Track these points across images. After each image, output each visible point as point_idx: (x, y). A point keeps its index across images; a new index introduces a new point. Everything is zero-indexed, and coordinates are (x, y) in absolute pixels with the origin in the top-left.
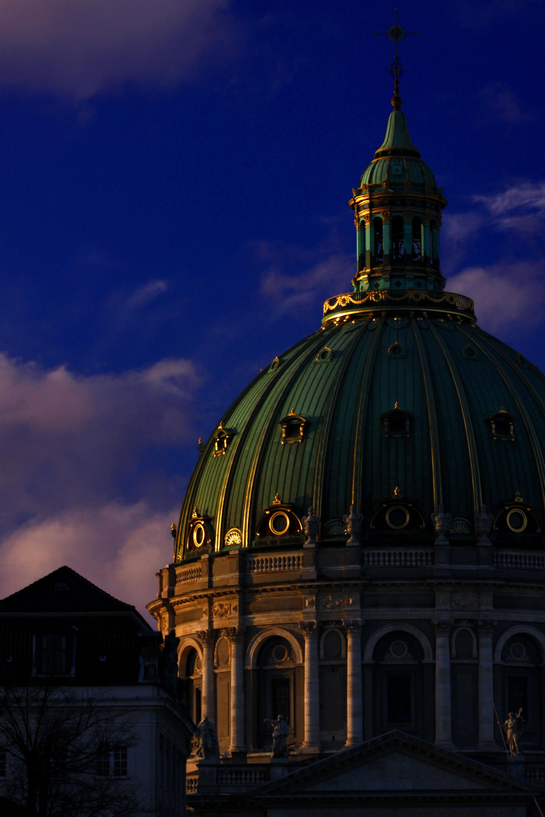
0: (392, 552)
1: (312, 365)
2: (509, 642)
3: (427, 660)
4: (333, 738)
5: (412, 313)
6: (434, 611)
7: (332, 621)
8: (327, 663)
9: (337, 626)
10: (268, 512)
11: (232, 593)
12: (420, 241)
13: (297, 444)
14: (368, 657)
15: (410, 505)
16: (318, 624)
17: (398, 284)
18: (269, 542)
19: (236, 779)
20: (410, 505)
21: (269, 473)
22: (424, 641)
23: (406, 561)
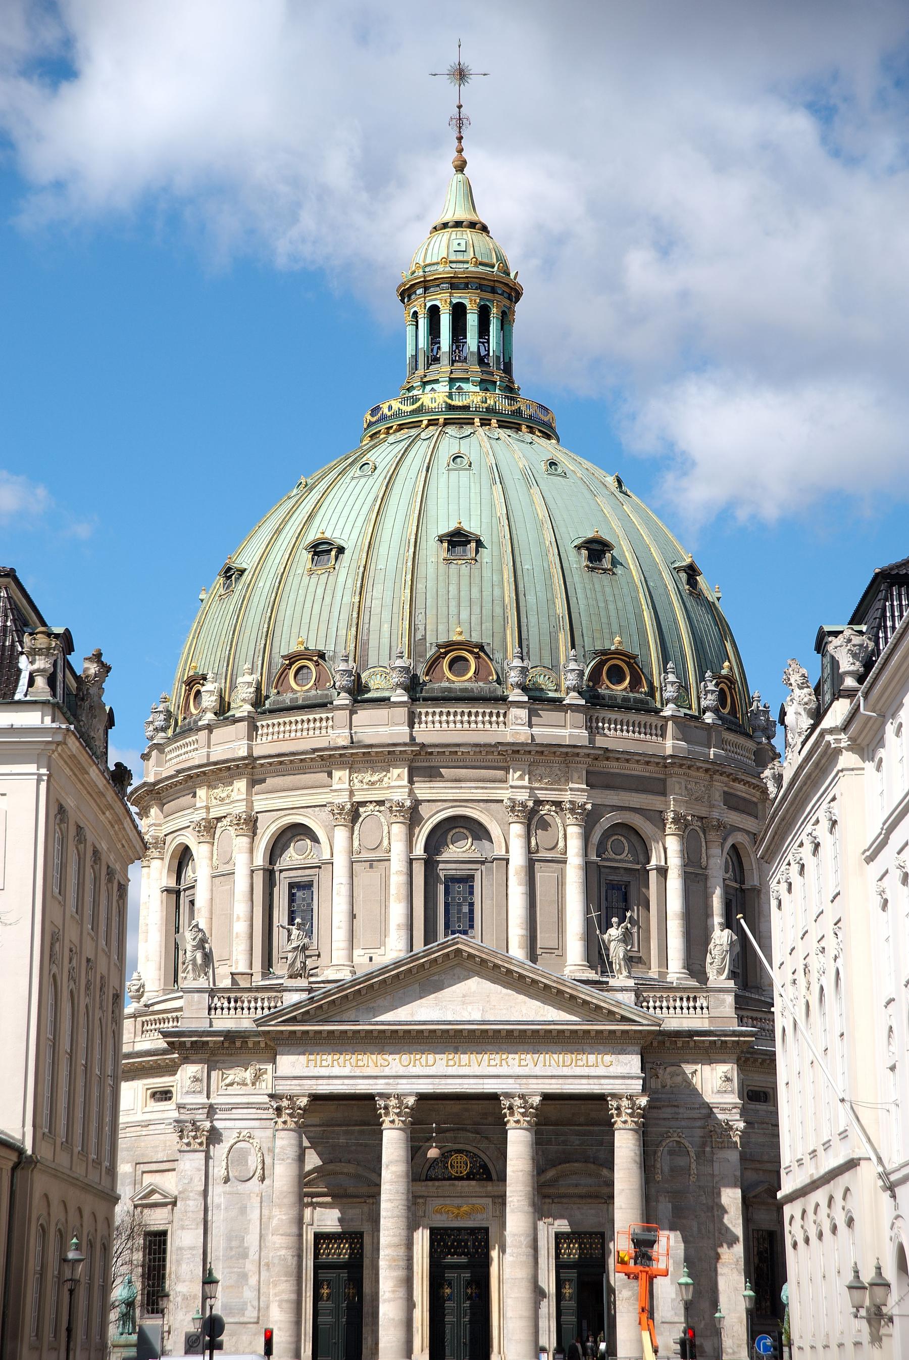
0: (452, 710)
1: (348, 480)
2: (607, 834)
3: (500, 851)
4: (371, 959)
5: (477, 420)
6: (507, 789)
7: (371, 802)
9: (377, 808)
10: (287, 662)
11: (237, 766)
12: (488, 342)
13: (327, 574)
14: (419, 850)
15: (476, 650)
16: (352, 805)
18: (288, 701)
19: (236, 1009)
20: (476, 650)
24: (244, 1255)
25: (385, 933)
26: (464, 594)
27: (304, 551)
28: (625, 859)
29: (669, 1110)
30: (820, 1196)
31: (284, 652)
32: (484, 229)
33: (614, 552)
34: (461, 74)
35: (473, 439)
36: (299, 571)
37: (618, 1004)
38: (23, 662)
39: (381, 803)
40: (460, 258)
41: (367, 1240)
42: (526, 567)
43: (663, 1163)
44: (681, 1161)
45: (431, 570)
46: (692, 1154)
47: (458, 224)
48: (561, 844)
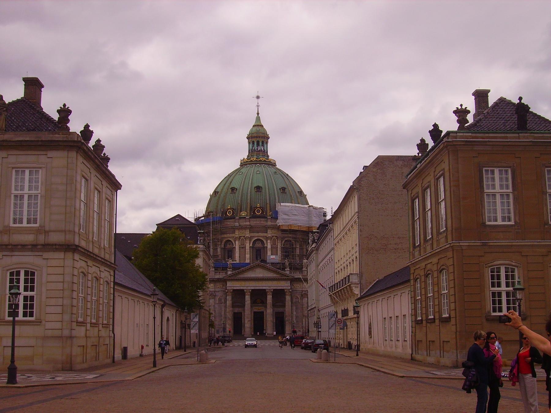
8: (241, 246)
14: (251, 245)
17: (258, 157)
21: (227, 201)
22: (265, 242)
23: (260, 222)
24: (222, 316)
25: (245, 260)
26: (259, 197)
27: (230, 189)
28: (288, 246)
29: (296, 291)
30: (312, 311)
31: (226, 208)
32: (263, 126)
33: (287, 189)
34: (258, 97)
35: (261, 167)
36: (229, 193)
37: (286, 274)
38: (199, 237)
39: (244, 236)
40: (258, 132)
41: (243, 314)
42: (271, 192)
43: (294, 300)
44: (297, 300)
45: (253, 193)
46: (299, 299)
47: (258, 125)
48: (277, 244)
